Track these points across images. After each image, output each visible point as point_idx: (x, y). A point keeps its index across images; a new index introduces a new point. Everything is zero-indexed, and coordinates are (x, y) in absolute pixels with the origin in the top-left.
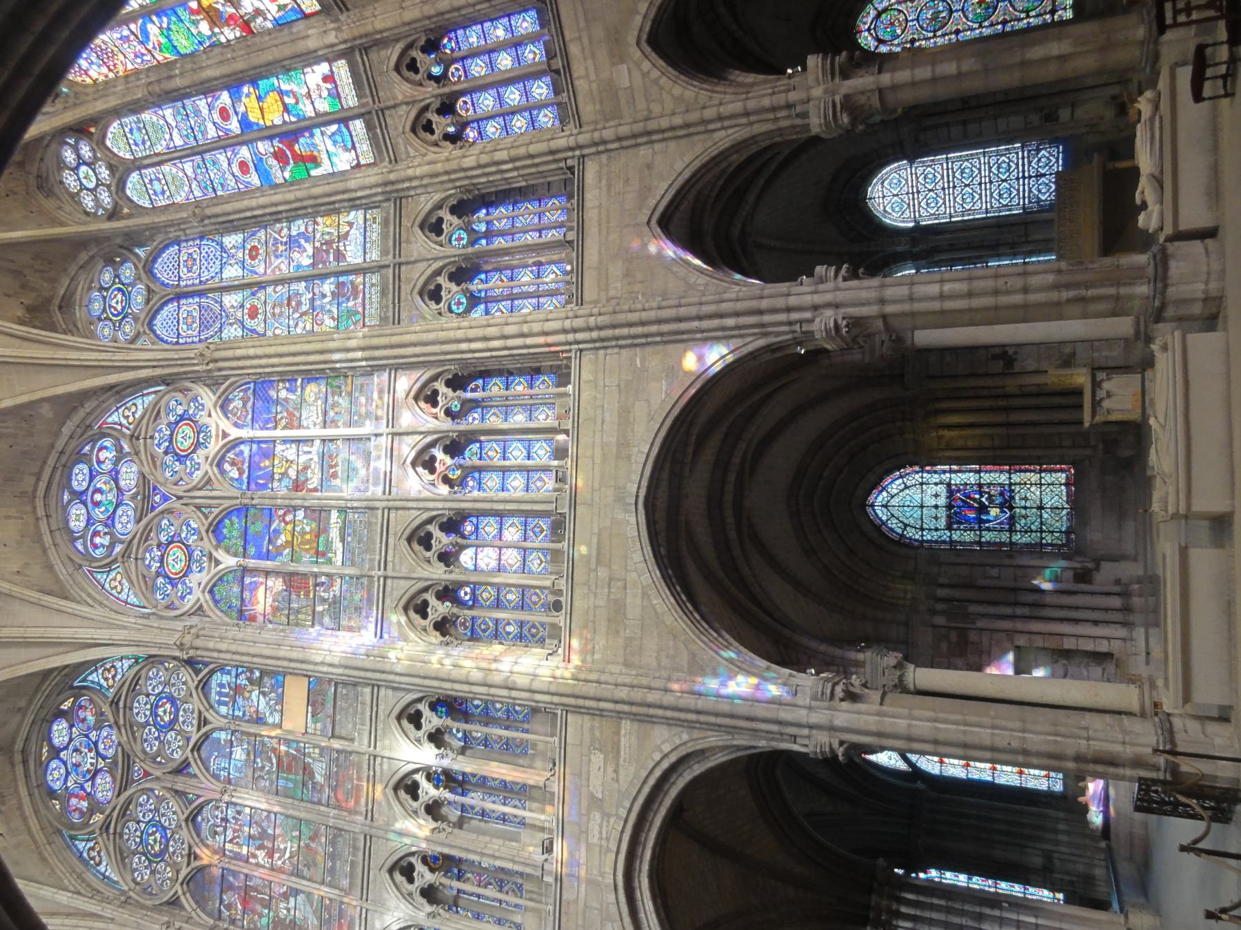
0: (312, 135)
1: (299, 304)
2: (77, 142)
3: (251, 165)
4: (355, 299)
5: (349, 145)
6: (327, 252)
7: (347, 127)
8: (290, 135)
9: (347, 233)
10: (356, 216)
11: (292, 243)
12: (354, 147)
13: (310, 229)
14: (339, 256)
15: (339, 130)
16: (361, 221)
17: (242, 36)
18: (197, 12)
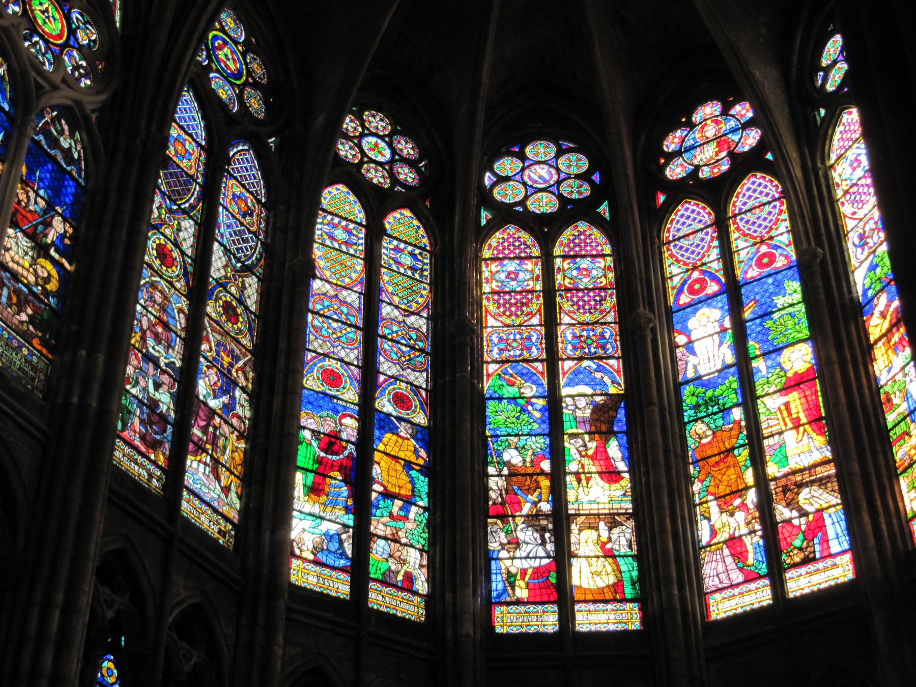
0: (347, 510)
1: (158, 339)
2: (418, 171)
3: (333, 392)
4: (143, 438)
5: (322, 557)
6: (205, 430)
7: (342, 570)
8: (358, 476)
9: (218, 478)
10: (232, 505)
11: (228, 385)
12: (316, 562)
13: (235, 421)
14: (200, 449)
15: (343, 555)
16: (225, 509)
17: (487, 498)
18: (535, 463)
